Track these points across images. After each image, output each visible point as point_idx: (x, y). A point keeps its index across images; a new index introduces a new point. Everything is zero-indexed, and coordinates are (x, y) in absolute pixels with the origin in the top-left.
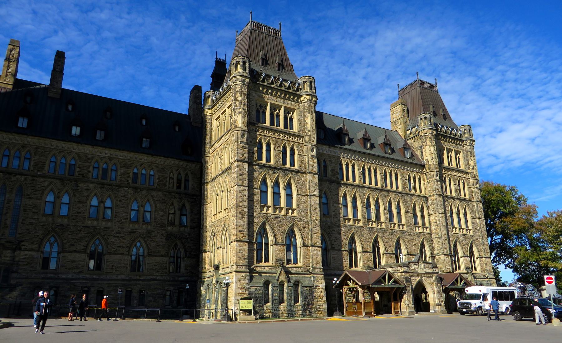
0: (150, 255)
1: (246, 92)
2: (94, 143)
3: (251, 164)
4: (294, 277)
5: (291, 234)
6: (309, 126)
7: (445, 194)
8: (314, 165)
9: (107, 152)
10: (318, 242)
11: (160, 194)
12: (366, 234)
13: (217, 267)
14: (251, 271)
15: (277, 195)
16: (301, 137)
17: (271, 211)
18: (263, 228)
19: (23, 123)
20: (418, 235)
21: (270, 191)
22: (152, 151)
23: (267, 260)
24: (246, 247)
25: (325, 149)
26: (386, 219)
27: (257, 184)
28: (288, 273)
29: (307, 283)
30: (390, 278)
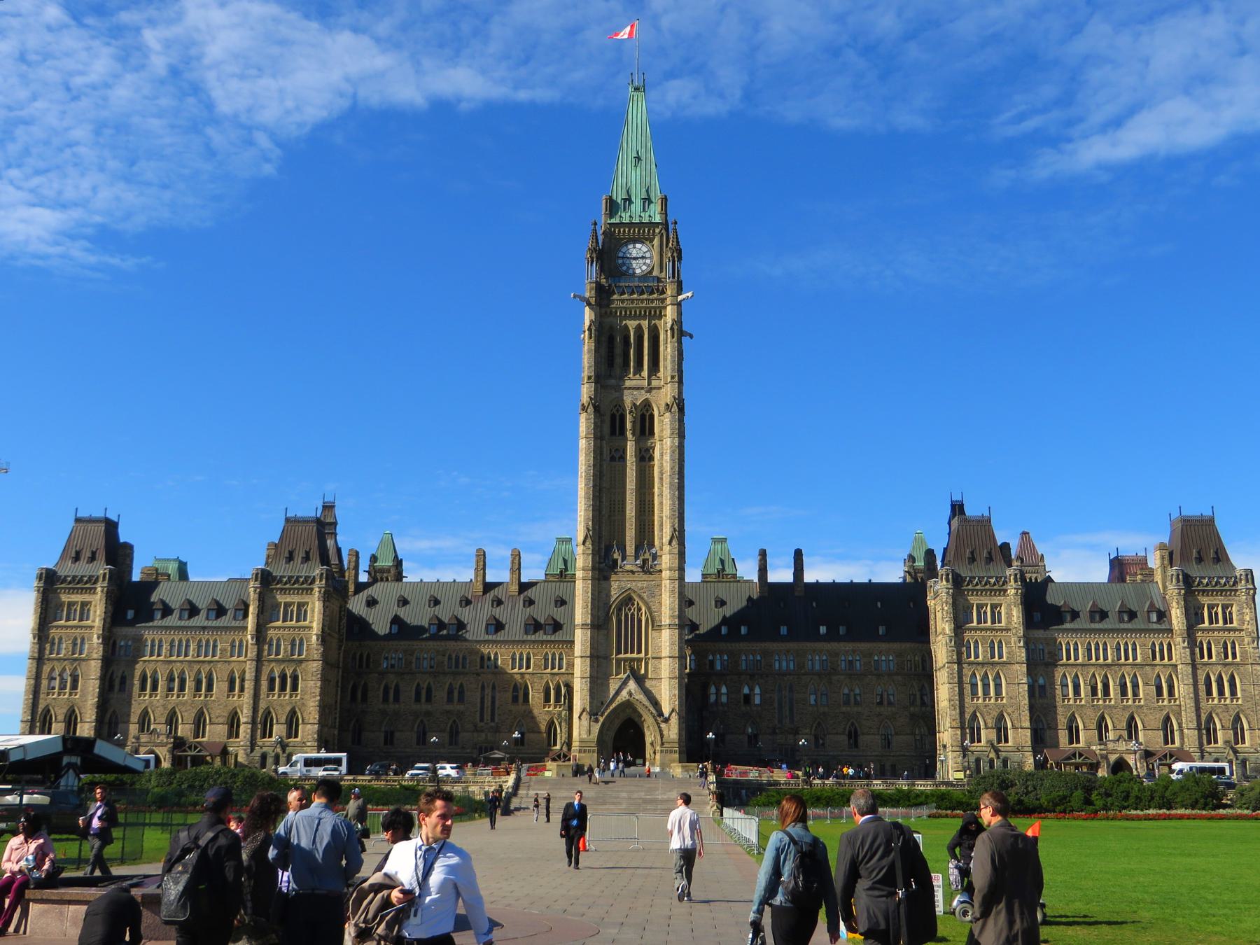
0: (897, 734)
1: (950, 601)
2: (839, 639)
3: (959, 663)
4: (1003, 754)
5: (1001, 718)
6: (1015, 619)
7: (1198, 660)
8: (1022, 655)
9: (849, 646)
10: (1027, 724)
11: (900, 678)
12: (1090, 712)
13: (945, 747)
14: (965, 750)
15: (986, 686)
16: (1008, 630)
17: (980, 701)
18: (974, 716)
19: (784, 630)
20: (1161, 709)
21: (980, 684)
22: (889, 637)
23: (979, 741)
24: (959, 732)
25: (1039, 634)
26: (1116, 694)
27: (967, 679)
28: (997, 751)
29: (1016, 759)
30: (1081, 755)
